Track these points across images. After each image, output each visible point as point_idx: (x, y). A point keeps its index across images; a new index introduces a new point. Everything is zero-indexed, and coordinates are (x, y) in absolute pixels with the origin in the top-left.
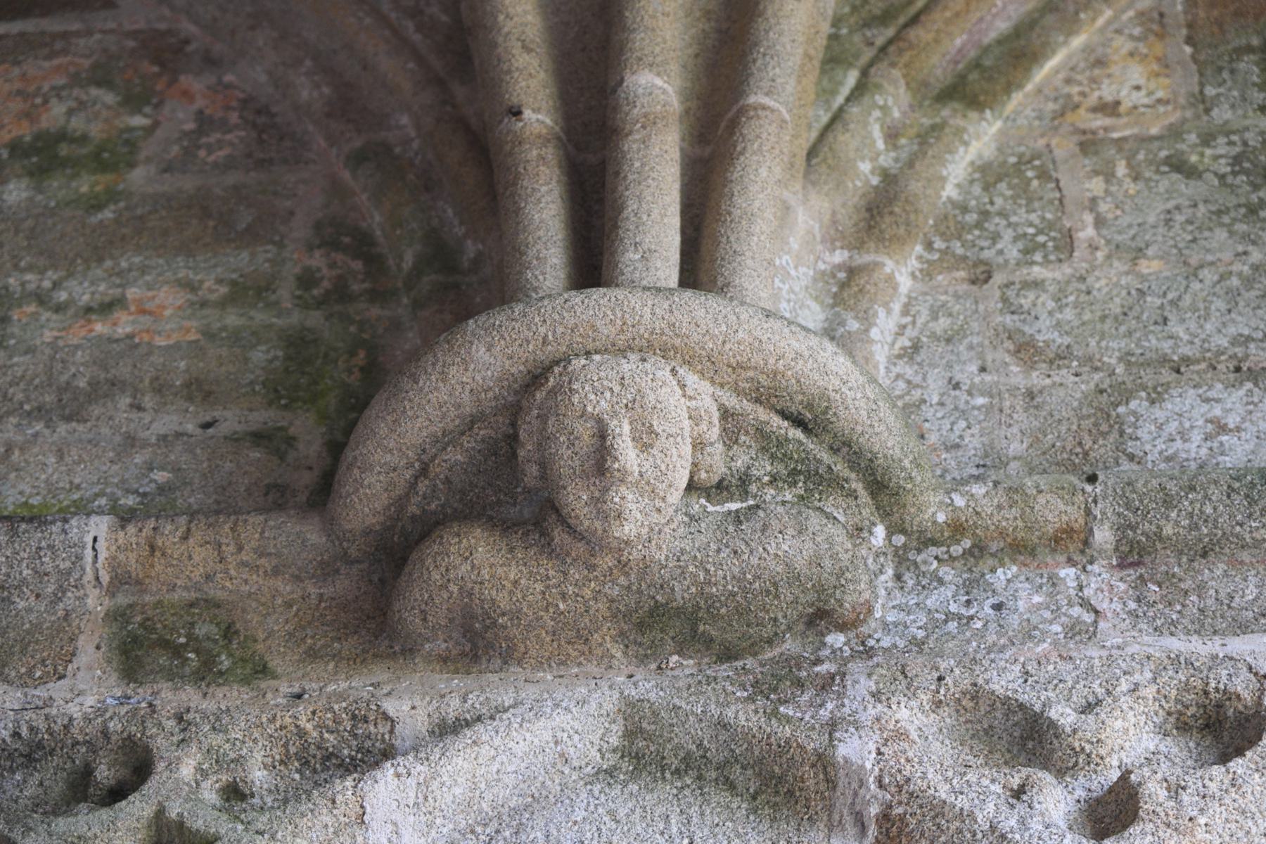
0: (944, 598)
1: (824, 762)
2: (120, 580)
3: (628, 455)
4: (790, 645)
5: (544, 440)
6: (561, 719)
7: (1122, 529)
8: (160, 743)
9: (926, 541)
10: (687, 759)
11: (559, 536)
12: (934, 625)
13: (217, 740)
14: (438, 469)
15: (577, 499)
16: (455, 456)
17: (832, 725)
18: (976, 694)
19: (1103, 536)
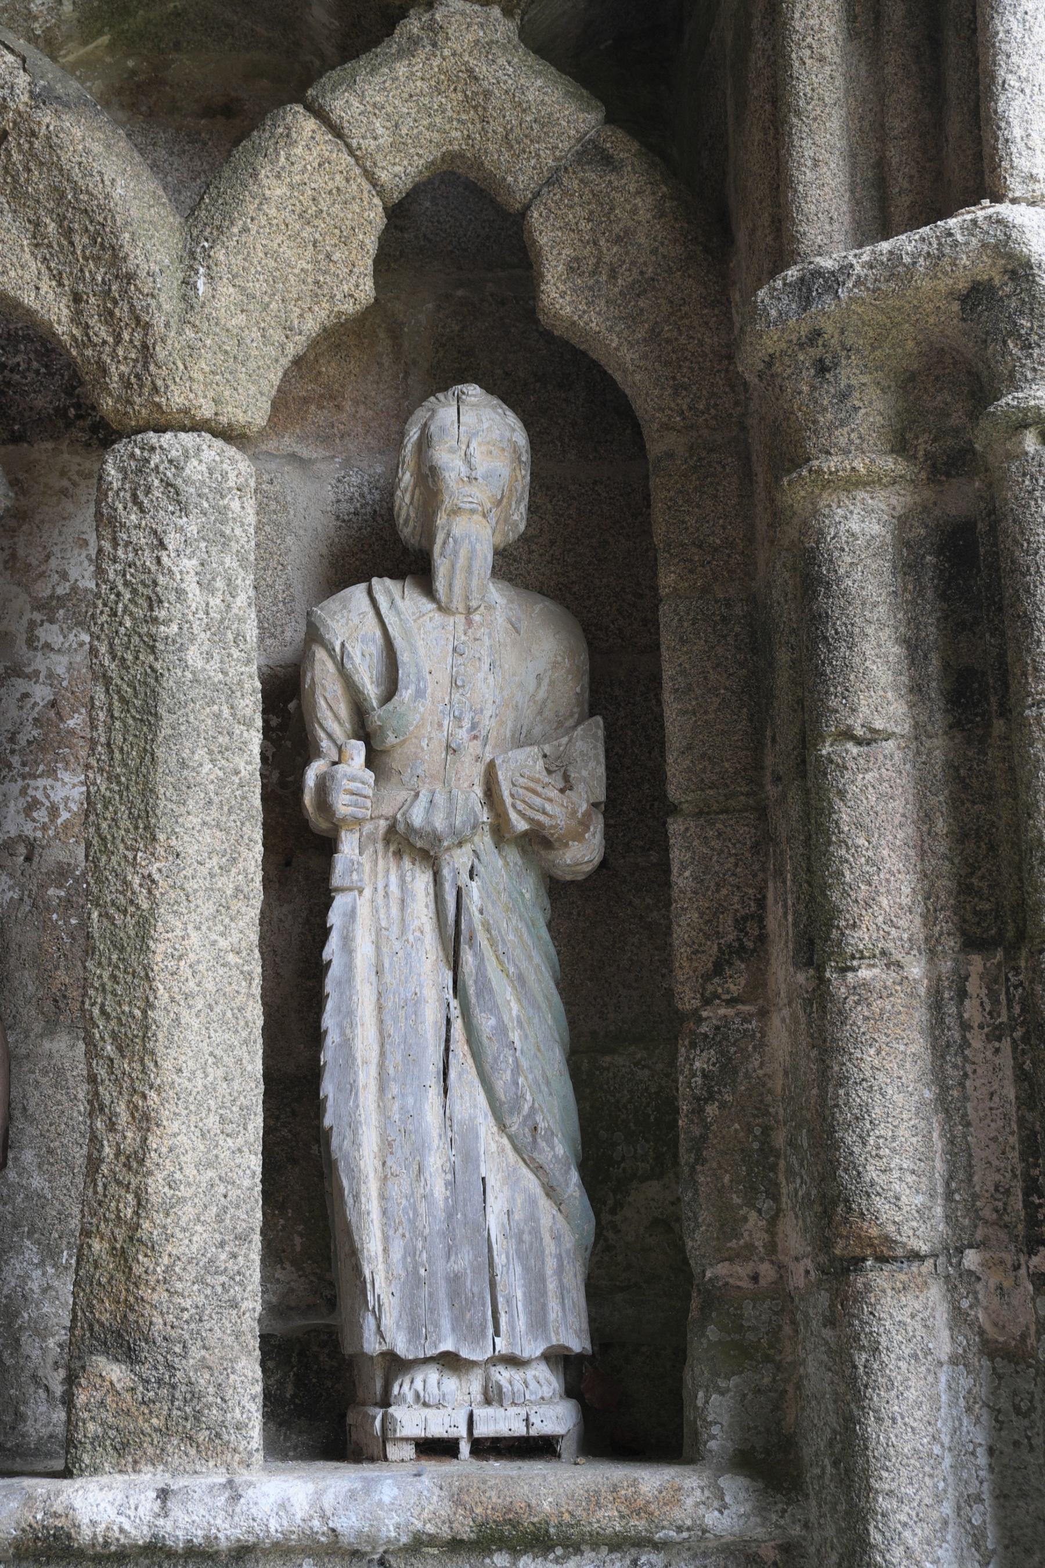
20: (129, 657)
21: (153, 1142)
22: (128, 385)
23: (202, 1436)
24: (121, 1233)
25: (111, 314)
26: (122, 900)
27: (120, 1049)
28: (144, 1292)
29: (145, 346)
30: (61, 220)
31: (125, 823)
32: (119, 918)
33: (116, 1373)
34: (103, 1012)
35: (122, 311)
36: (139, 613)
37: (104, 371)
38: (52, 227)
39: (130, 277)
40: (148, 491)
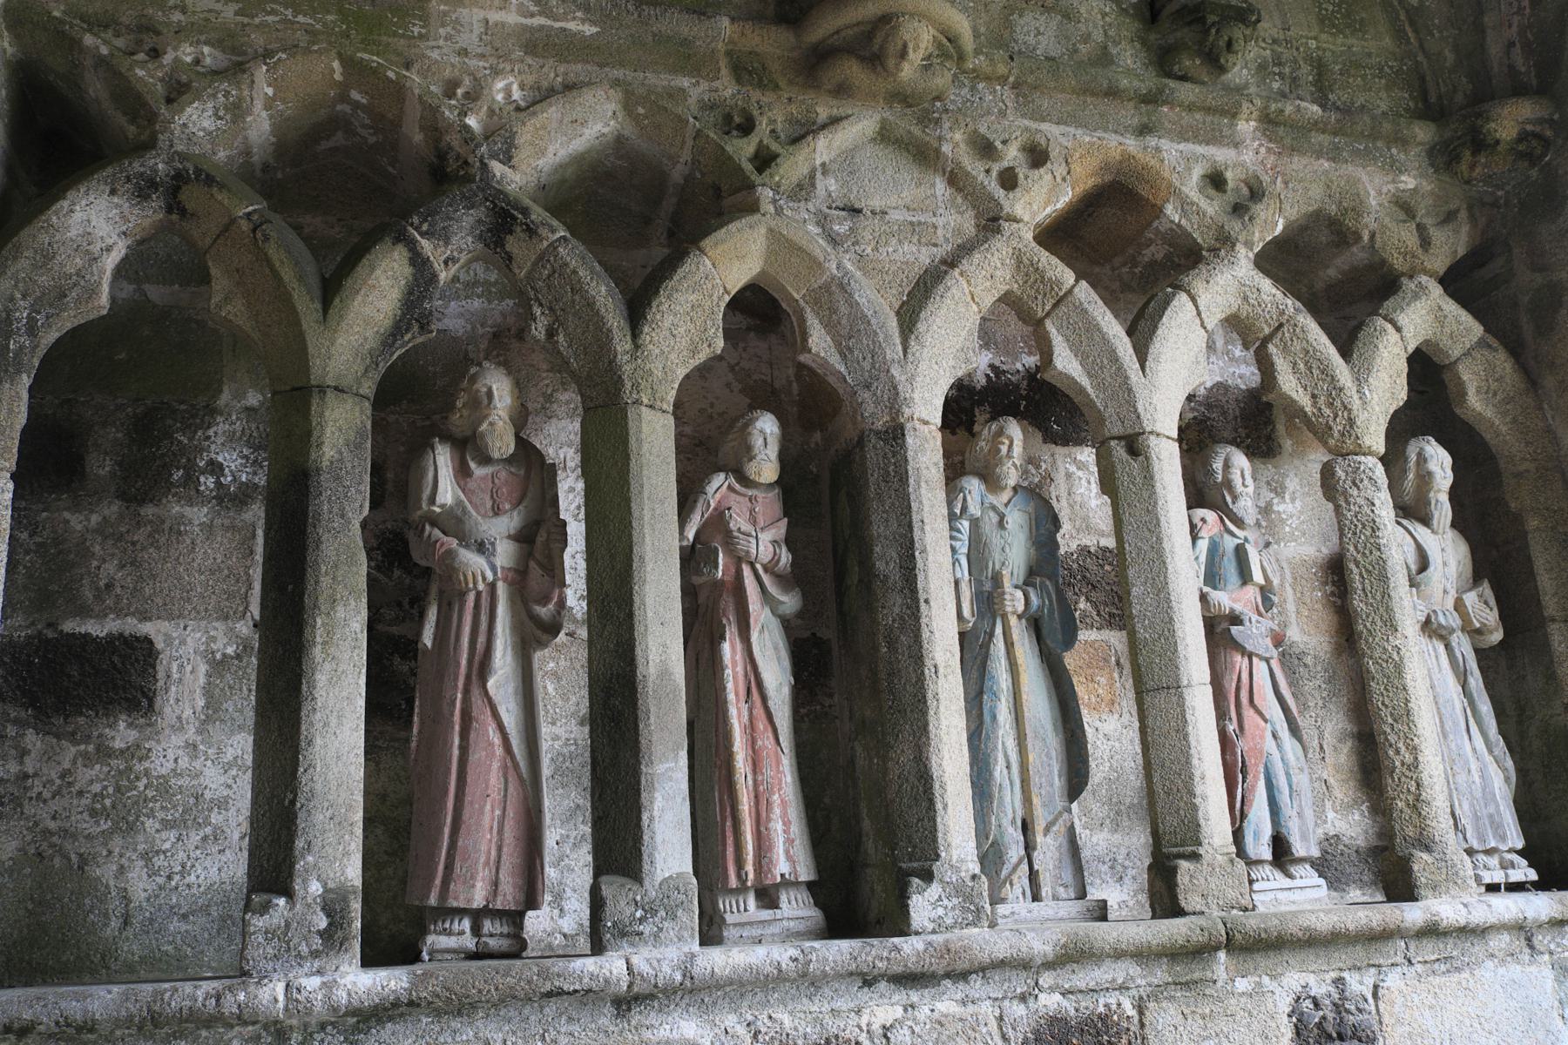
0: (965, 91)
1: (938, 151)
2: (731, 41)
3: (911, 55)
4: (926, 105)
5: (885, 40)
6: (865, 122)
7: (1017, 78)
8: (756, 113)
9: (964, 72)
10: (897, 140)
11: (879, 68)
12: (964, 103)
13: (770, 114)
14: (843, 34)
15: (891, 62)
16: (850, 32)
17: (940, 138)
18: (975, 131)
19: (1011, 79)
20: (1367, 552)
21: (1420, 759)
22: (1343, 435)
23: (1459, 882)
24: (1411, 798)
25: (1332, 404)
26: (1384, 657)
27: (1395, 720)
28: (1428, 822)
29: (1350, 419)
30: (1306, 363)
31: (1379, 623)
32: (1384, 665)
33: (1425, 856)
34: (1383, 704)
35: (1338, 403)
36: (1368, 534)
37: (1331, 428)
38: (1302, 366)
39: (1341, 390)
40: (1362, 481)
